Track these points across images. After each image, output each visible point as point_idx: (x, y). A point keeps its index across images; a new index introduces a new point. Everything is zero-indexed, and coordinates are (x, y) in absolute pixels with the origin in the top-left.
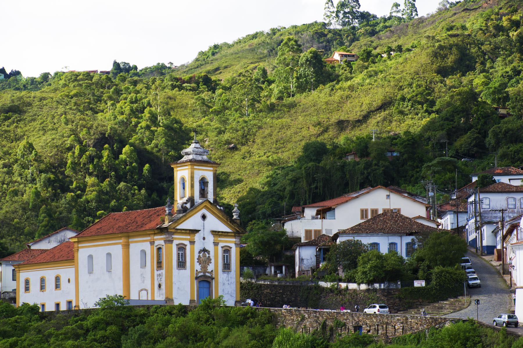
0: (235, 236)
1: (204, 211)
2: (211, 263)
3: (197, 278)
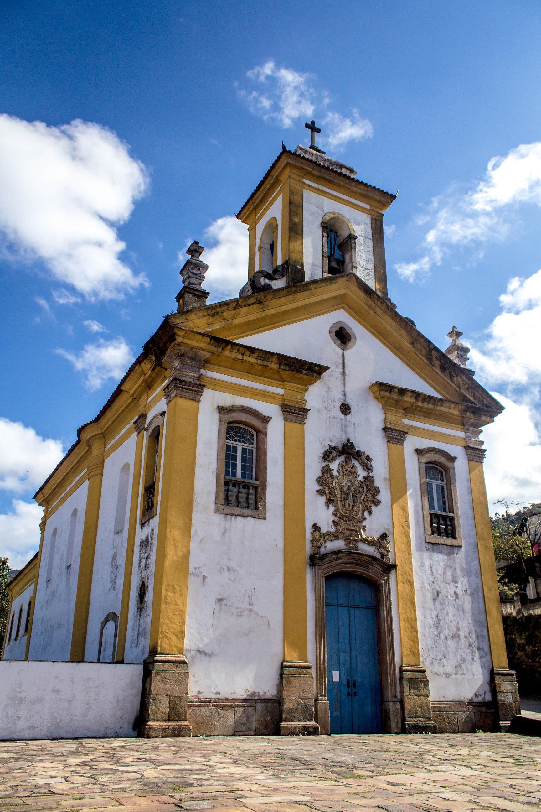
2: (377, 503)
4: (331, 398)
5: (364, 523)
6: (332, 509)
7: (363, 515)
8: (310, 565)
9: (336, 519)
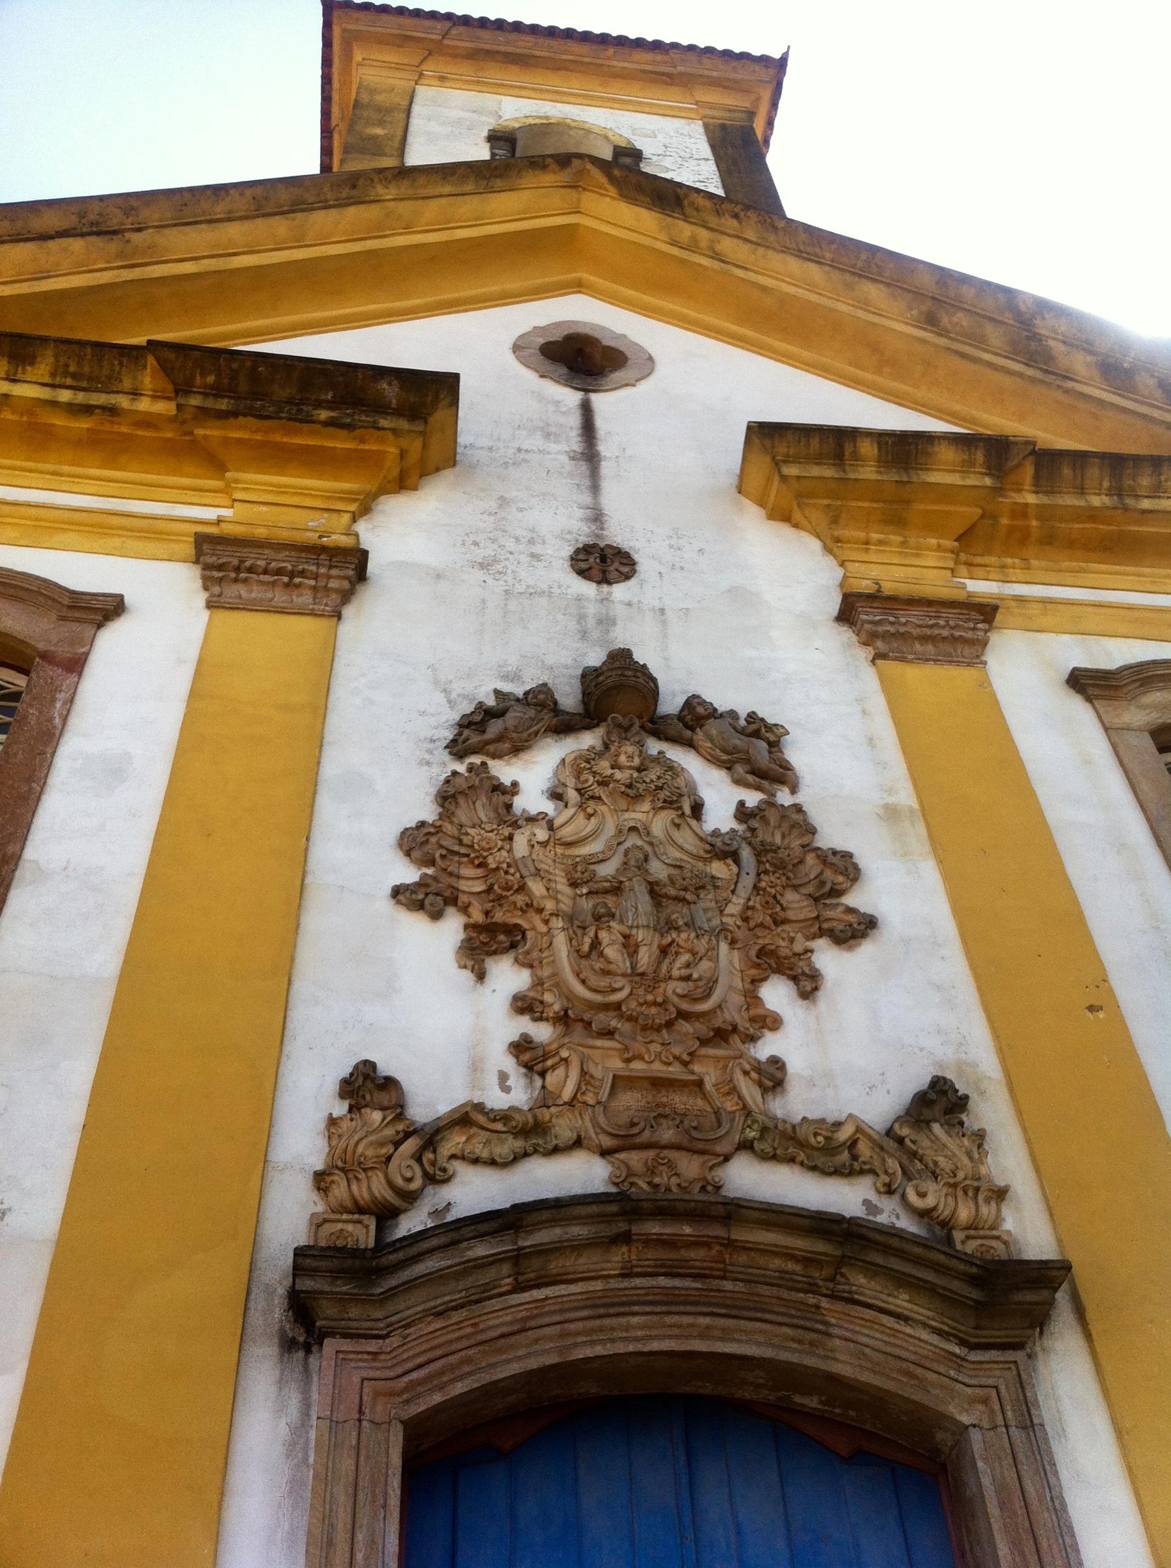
2: (857, 930)
3: (335, 1293)
4: (520, 532)
5: (767, 1047)
6: (508, 976)
7: (752, 998)
8: (288, 1345)
9: (542, 1032)
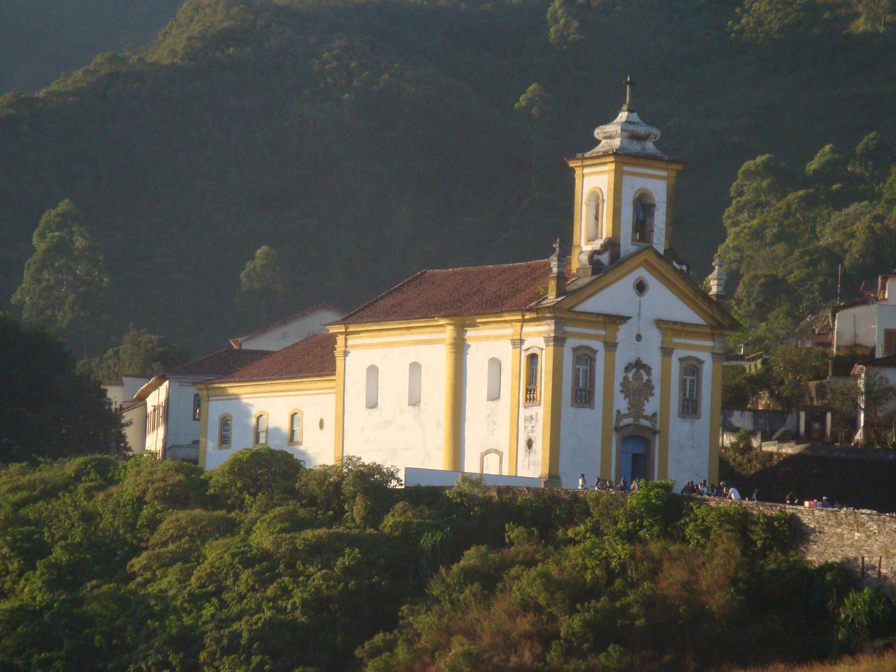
0: (712, 336)
1: (642, 273)
2: (652, 395)
6: (627, 400)
